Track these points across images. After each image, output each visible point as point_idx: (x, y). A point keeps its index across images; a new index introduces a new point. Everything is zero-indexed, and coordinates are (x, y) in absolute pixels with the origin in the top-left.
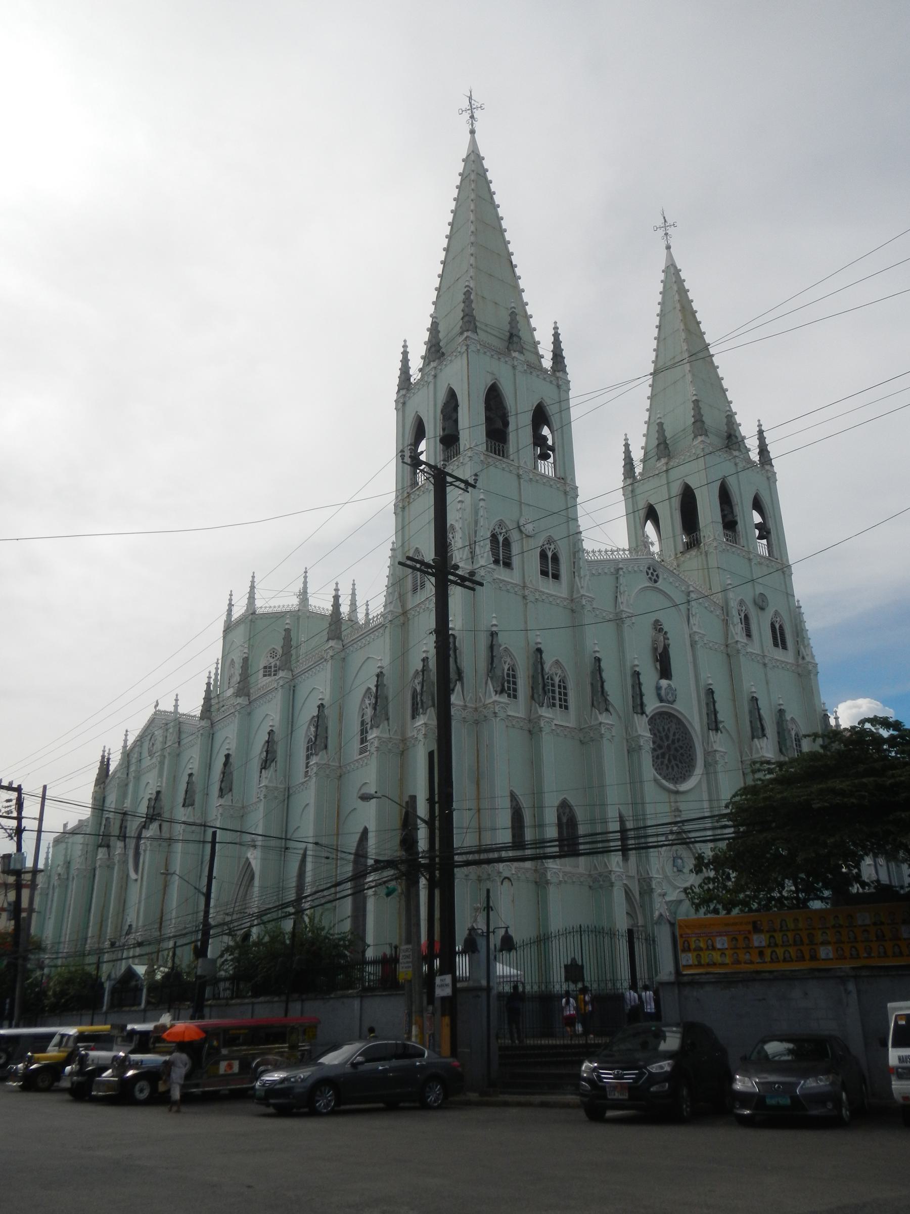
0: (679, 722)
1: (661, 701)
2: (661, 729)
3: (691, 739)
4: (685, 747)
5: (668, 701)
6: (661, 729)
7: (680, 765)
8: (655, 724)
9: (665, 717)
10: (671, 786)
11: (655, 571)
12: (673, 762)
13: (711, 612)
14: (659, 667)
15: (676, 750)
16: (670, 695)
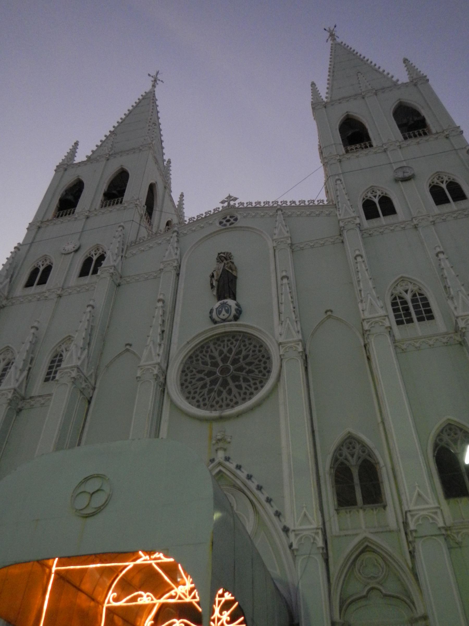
0: (250, 337)
1: (215, 322)
2: (216, 354)
3: (267, 351)
4: (256, 362)
5: (222, 319)
6: (216, 354)
7: (244, 385)
8: (207, 352)
9: (226, 339)
10: (215, 414)
11: (231, 217)
12: (232, 385)
13: (318, 215)
14: (215, 293)
15: (241, 369)
16: (224, 312)
